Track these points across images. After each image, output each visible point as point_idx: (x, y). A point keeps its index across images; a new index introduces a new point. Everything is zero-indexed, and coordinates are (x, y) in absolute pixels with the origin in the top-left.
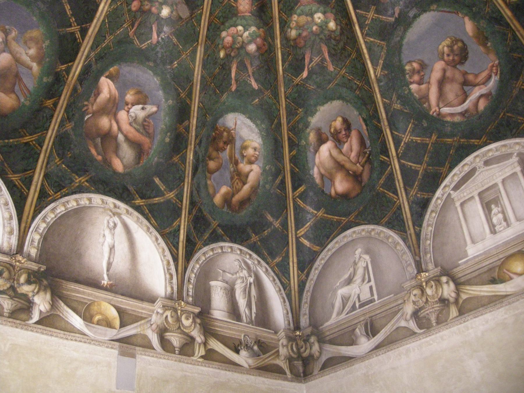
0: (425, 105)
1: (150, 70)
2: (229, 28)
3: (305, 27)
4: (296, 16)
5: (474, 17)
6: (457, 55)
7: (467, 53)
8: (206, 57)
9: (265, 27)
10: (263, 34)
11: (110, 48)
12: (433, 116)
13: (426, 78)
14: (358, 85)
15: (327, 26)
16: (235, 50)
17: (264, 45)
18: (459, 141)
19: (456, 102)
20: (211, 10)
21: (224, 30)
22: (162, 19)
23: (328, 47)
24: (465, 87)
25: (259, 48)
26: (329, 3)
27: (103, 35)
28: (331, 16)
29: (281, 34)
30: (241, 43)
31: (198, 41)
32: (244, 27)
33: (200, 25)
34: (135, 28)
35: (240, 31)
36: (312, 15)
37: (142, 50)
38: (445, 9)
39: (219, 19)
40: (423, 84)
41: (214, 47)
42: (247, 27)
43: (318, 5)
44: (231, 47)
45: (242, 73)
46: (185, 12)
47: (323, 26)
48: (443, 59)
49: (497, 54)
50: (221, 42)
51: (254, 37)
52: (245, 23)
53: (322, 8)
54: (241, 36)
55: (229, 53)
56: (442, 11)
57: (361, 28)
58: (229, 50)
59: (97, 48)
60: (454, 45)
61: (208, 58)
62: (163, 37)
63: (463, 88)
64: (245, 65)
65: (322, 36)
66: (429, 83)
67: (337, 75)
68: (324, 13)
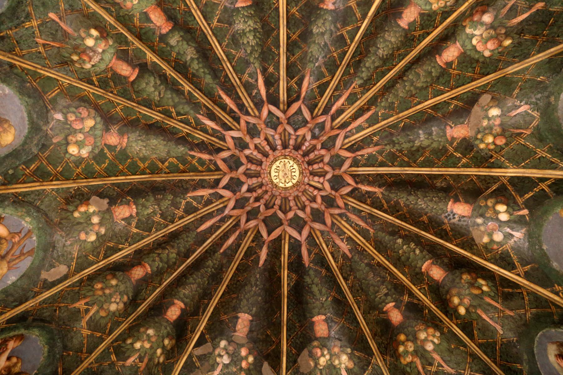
2: (479, 52)
4: (433, 7)
8: (517, 60)
10: (467, 21)
11: (550, 147)
16: (498, 31)
17: (477, 11)
20: (469, 83)
21: (483, 56)
22: (502, 111)
27: (538, 161)
29: (455, 11)
30: (488, 31)
32: (471, 39)
33: (488, 83)
34: (522, 131)
35: (477, 39)
37: (541, 114)
39: (475, 68)
41: (503, 56)
44: (496, 37)
45: (519, 8)
46: (485, 99)
50: (496, 52)
52: (467, 40)
55: (503, 36)
58: (501, 38)
59: (553, 163)
61: (517, 56)
62: (519, 102)
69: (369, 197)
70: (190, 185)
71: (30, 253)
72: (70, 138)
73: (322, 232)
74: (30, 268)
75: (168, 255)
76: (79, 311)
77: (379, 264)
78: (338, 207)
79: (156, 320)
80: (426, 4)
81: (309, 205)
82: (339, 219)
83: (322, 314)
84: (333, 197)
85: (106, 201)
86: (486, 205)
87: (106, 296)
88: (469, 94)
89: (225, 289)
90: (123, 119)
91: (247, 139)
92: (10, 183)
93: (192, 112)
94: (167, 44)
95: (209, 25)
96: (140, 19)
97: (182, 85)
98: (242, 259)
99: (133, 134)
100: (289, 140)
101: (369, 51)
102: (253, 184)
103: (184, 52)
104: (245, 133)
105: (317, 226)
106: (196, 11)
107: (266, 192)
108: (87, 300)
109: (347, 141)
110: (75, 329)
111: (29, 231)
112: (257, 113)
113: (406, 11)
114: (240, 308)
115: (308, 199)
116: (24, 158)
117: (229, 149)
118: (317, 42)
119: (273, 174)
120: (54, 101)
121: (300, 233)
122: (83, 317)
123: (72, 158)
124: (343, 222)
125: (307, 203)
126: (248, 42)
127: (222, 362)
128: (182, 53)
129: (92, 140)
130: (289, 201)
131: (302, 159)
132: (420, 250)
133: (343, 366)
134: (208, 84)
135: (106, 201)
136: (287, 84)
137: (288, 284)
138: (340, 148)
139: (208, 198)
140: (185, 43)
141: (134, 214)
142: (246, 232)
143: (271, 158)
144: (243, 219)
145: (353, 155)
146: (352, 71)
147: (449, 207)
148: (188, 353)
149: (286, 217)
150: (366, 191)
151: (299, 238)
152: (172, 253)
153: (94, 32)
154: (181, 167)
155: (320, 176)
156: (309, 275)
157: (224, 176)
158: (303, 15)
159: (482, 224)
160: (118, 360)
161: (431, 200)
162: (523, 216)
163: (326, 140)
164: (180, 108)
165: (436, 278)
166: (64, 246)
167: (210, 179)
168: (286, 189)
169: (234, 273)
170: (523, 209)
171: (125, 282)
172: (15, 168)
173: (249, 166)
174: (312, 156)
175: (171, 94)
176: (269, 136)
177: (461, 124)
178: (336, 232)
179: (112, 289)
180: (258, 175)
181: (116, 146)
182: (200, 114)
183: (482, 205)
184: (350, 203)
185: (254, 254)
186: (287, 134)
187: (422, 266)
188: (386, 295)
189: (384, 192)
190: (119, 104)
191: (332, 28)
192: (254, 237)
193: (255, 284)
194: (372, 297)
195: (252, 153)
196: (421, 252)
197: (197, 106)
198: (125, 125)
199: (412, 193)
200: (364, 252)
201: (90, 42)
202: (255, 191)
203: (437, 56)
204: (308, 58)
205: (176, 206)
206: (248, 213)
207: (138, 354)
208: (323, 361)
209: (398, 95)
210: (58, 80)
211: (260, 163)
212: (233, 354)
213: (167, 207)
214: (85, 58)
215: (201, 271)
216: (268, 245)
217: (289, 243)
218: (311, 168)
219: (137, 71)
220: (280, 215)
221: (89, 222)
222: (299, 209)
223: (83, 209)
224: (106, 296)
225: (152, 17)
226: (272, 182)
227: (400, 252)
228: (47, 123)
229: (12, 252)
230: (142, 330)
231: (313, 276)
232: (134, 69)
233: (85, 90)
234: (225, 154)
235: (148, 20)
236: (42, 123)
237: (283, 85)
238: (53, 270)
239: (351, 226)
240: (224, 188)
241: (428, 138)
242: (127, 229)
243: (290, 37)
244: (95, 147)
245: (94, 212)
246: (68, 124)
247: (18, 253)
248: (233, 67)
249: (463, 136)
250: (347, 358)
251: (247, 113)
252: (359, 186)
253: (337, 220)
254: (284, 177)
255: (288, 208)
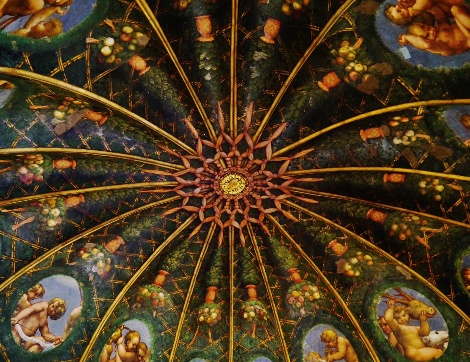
0: (15, 311)
1: (4, 107)
3: (46, 204)
5: (84, 312)
6: (55, 311)
7: (59, 318)
9: (45, 181)
12: (10, 322)
13: (34, 301)
14: (11, 256)
15: (50, 219)
18: (3, 352)
19: (27, 331)
23: (32, 223)
24: (38, 330)
25: (23, 175)
26: (69, 218)
28: (59, 221)
31: (39, 146)
32: (42, 164)
36: (57, 206)
38: (82, 292)
40: (29, 301)
42: (43, 166)
43: (65, 210)
47: (48, 216)
48: (50, 304)
49: (68, 338)
51: (33, 171)
53: (63, 213)
54: (34, 163)
56: (80, 290)
57: (61, 250)
60: (61, 306)
63: (37, 329)
64: (7, 167)
65: (41, 216)
66: (31, 305)
67: (10, 234)
68: (60, 216)
69: (198, 124)
70: (289, 226)
71: (398, 290)
72: (311, 300)
73: (252, 135)
74: (408, 286)
75: (350, 207)
76: (431, 240)
77: (239, 81)
78: (224, 138)
79: (409, 186)
80: (59, 201)
81: (240, 156)
82: (232, 133)
83: (318, 85)
84: (221, 147)
85: (337, 263)
86: (116, 58)
87: (410, 226)
88: (70, 144)
89: (348, 167)
90: (280, 279)
91: (233, 217)
92: (354, 327)
93: (245, 250)
94: (220, 282)
95: (191, 280)
96: (219, 302)
97: (234, 267)
98: (317, 168)
99: (285, 268)
100: (211, 197)
101: (116, 199)
102: (258, 195)
103: (216, 272)
104: (230, 221)
105: (250, 142)
106: (190, 292)
107: (255, 185)
108: (418, 238)
109: (177, 170)
110: (447, 234)
111: (383, 297)
112: (213, 223)
113: (75, 204)
114: (358, 142)
115: (237, 160)
116: (337, 321)
117: (248, 222)
118: (143, 226)
119: (240, 190)
120: (296, 319)
121: (265, 147)
122: (435, 233)
123: (322, 294)
124: (232, 129)
125: (240, 159)
126: (180, 254)
127: (414, 135)
128: (218, 273)
129: (305, 288)
130: (249, 169)
131: (215, 182)
132: (199, 56)
133: (351, 49)
134: (222, 252)
135: (337, 263)
136: (180, 225)
137: (311, 134)
138: (186, 169)
139: (290, 210)
140: (211, 276)
141: (336, 240)
142: (294, 177)
143: (231, 198)
144: (286, 184)
145: (182, 157)
146: (137, 200)
147: (147, 70)
148: (417, 171)
149: (261, 164)
150: (196, 129)
151: (270, 145)
152: (347, 205)
153: (245, 315)
154: (282, 237)
155: (216, 165)
156: (293, 116)
157: (267, 214)
158: (139, 248)
159: (132, 44)
160: (460, 197)
161: (156, 83)
162: (93, 37)
163: (190, 180)
164: (249, 256)
165: (209, 22)
166: (383, 271)
167: (276, 219)
168: (243, 176)
169: (331, 167)
170: (89, 44)
171: (391, 219)
172: (345, 325)
173: (247, 205)
174: (207, 179)
175: (245, 265)
176: (220, 208)
177: (90, 120)
178: (243, 127)
179: (401, 224)
180: (249, 196)
181: (299, 273)
182: (242, 246)
183: (120, 59)
184: (214, 135)
185: (308, 160)
186: (208, 201)
187: (209, 42)
188: (259, 50)
189: (185, 117)
190: (272, 290)
191: (128, 226)
192: (294, 170)
193: (330, 142)
194: (271, 62)
195: (239, 208)
196: (200, 54)
197: (239, 253)
198: (283, 275)
199: (165, 100)
200: (240, 97)
201: (252, 314)
202: (261, 190)
203: (74, 168)
204: (156, 222)
205: (311, 223)
206: (279, 184)
207: (448, 184)
208: (359, 68)
209: (120, 166)
210: (282, 326)
211: (241, 201)
212: (402, 130)
213: (316, 226)
214: (262, 313)
215: (348, 179)
216: (292, 156)
217: (278, 150)
218: (216, 173)
219: (247, 286)
220: (263, 167)
221: (359, 264)
222: (249, 160)
223: (351, 273)
224: (410, 226)
225: (213, 298)
226: (247, 186)
227: (215, 69)
228: (310, 316)
229: (402, 301)
230: (424, 192)
231: (291, 113)
232: (248, 288)
233: (277, 311)
234: (253, 220)
235: (216, 299)
236: (312, 318)
237: (183, 227)
238: (403, 273)
239: (229, 122)
240: (274, 207)
241: (122, 126)
242: (349, 241)
243: (155, 244)
244: (307, 284)
245: (349, 264)
246: (304, 304)
247: (401, 297)
248: (200, 252)
249: (95, 113)
250: (342, 48)
251: (218, 227)
252: (197, 136)
253: (234, 134)
254: (236, 184)
255: (255, 166)
